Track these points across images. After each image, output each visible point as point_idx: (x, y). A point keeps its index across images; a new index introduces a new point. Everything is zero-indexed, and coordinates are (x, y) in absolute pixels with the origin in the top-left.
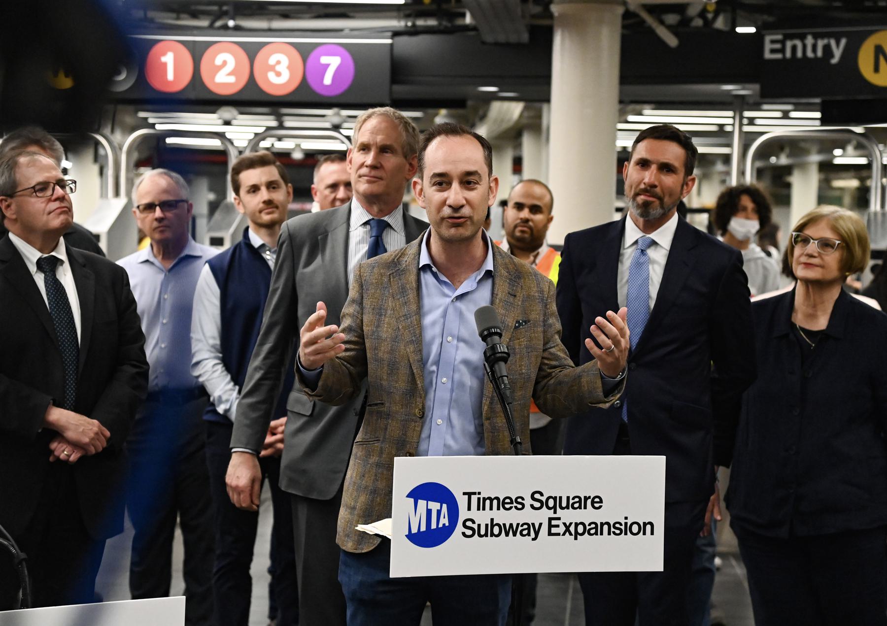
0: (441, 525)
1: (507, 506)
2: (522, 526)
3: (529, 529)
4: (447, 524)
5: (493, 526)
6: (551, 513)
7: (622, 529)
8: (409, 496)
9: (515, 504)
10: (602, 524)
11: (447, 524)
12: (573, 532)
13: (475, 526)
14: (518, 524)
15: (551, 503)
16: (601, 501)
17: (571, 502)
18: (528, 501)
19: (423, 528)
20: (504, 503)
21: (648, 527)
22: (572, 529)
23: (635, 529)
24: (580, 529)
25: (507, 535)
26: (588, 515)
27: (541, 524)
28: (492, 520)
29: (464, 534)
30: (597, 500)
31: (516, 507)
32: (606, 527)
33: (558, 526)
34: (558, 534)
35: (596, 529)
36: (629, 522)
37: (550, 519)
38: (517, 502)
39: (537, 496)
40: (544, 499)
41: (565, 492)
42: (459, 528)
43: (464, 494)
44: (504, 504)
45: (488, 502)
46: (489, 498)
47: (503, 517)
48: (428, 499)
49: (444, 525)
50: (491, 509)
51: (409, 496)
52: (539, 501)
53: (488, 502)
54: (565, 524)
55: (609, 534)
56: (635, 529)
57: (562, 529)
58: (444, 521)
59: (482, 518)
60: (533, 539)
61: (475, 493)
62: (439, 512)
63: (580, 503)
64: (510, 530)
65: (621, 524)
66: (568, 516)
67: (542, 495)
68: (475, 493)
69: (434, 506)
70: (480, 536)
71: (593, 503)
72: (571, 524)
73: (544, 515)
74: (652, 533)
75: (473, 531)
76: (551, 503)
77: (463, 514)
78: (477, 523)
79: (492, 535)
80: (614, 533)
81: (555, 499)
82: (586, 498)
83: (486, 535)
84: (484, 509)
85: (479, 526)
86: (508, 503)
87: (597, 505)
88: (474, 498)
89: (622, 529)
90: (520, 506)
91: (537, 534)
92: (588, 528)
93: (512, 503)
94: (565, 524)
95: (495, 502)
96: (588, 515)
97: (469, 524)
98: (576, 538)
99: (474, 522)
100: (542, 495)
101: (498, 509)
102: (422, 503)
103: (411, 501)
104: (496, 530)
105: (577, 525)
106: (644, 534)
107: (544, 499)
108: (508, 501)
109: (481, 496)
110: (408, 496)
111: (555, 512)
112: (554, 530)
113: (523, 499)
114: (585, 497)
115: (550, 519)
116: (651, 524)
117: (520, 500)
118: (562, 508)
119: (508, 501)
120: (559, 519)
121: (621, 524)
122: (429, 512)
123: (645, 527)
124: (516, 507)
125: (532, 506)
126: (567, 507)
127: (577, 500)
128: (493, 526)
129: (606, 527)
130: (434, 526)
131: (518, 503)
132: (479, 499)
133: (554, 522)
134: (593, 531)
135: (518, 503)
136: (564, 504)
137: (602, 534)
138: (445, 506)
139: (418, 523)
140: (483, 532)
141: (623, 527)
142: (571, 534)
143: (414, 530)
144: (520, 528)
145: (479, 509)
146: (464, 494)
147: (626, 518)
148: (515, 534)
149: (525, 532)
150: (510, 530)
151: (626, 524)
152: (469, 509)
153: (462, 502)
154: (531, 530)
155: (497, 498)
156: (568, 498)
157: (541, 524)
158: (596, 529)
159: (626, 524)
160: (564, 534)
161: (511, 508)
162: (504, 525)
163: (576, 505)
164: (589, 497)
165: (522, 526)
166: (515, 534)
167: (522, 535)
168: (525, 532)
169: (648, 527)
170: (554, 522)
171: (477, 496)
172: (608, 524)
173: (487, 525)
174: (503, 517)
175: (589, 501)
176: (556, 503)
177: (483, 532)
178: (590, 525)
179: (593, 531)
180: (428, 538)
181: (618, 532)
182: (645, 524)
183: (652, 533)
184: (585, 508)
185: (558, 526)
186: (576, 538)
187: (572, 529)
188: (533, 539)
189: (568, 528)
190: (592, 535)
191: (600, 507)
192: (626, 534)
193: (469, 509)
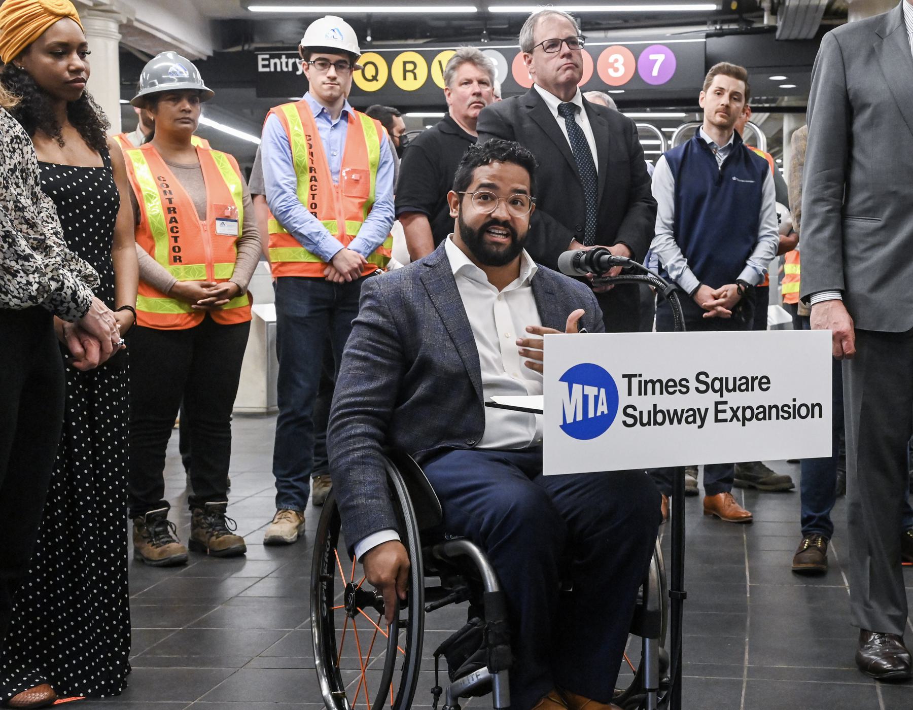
0: (599, 414)
1: (671, 390)
2: (687, 412)
3: (694, 415)
4: (606, 412)
5: (656, 413)
6: (717, 397)
7: (789, 412)
8: (562, 379)
9: (679, 388)
10: (770, 408)
11: (606, 412)
12: (741, 418)
13: (637, 414)
14: (683, 410)
15: (717, 385)
16: (768, 382)
17: (738, 383)
18: (693, 384)
19: (580, 417)
20: (667, 386)
21: (817, 409)
22: (740, 414)
23: (803, 411)
24: (748, 414)
25: (671, 422)
26: (755, 398)
27: (707, 410)
28: (655, 406)
29: (625, 423)
30: (764, 380)
31: (680, 391)
32: (774, 411)
33: (724, 411)
34: (725, 420)
35: (764, 413)
36: (798, 404)
37: (717, 404)
38: (681, 385)
39: (702, 377)
40: (709, 381)
41: (731, 372)
42: (620, 417)
43: (624, 376)
44: (667, 387)
45: (650, 385)
46: (652, 381)
47: (667, 402)
48: (584, 383)
49: (603, 412)
50: (654, 393)
51: (562, 379)
52: (705, 382)
53: (650, 385)
54: (732, 408)
55: (778, 418)
56: (803, 411)
57: (729, 414)
58: (603, 408)
59: (644, 404)
60: (700, 427)
61: (635, 376)
62: (597, 398)
63: (747, 384)
64: (674, 417)
65: (789, 407)
66: (735, 399)
67: (707, 376)
68: (635, 376)
69: (591, 391)
70: (643, 424)
71: (760, 383)
72: (738, 408)
73: (711, 398)
74: (820, 416)
75: (635, 420)
76: (717, 385)
77: (624, 400)
78: (639, 410)
79: (656, 423)
80: (782, 416)
81: (721, 380)
82: (753, 379)
83: (649, 423)
84: (646, 394)
85: (641, 413)
86: (671, 386)
87: (764, 386)
88: (635, 381)
89: (789, 412)
90: (684, 390)
91: (703, 420)
92: (756, 412)
93: (675, 386)
94: (732, 408)
95: (658, 385)
96: (755, 398)
97: (630, 411)
98: (744, 425)
99: (635, 409)
100: (707, 376)
101: (661, 393)
102: (577, 388)
103: (565, 385)
104: (660, 418)
105: (744, 409)
106: (813, 416)
107: (709, 381)
108: (671, 383)
109: (643, 379)
111: (722, 396)
112: (721, 416)
113: (688, 381)
114: (752, 377)
115: (717, 404)
116: (819, 405)
117: (684, 383)
118: (729, 391)
119: (671, 383)
120: (726, 403)
121: (789, 407)
122: (585, 398)
123: (813, 409)
124: (680, 391)
125: (697, 389)
126: (734, 390)
127: (744, 381)
128: (656, 413)
129: (774, 411)
130: (591, 415)
131: (682, 386)
132: (640, 382)
133: (720, 407)
134: (761, 416)
135: (682, 386)
136: (731, 387)
137: (770, 418)
138: (603, 391)
139: (574, 413)
140: (645, 420)
141: (791, 410)
142: (738, 420)
143: (570, 420)
144: (685, 415)
145: (640, 394)
146: (624, 376)
147: (794, 400)
149: (690, 419)
150: (674, 417)
151: (794, 406)
152: (630, 394)
153: (621, 385)
154: (697, 417)
155: (660, 381)
156: (735, 379)
157: (707, 410)
158: (764, 413)
159: (794, 406)
160: (731, 420)
161: (675, 391)
162: (668, 411)
163: (743, 387)
164: (757, 378)
166: (679, 422)
167: (687, 422)
168: (690, 419)
169: (817, 409)
170: (720, 407)
171: (638, 379)
172: (776, 407)
173: (649, 412)
174: (667, 402)
175: (756, 382)
176: (722, 386)
177: (645, 420)
178: (757, 409)
179: (761, 416)
180: (585, 428)
181: (786, 415)
182: (813, 406)
183: (820, 416)
184: (753, 390)
185: (724, 411)
186: (744, 425)
187: (740, 414)
188: (700, 427)
189: (735, 412)
190: (760, 420)
191: (768, 388)
192: (794, 417)
193: (630, 394)
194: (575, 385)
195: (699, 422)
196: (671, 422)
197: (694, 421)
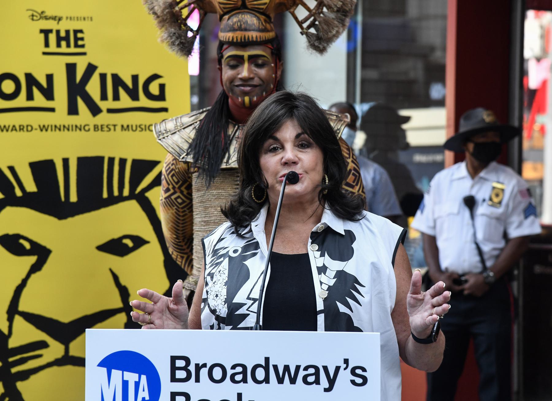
2: (306, 369)
3: (317, 374)
4: (147, 398)
8: (101, 365)
14: (298, 368)
48: (124, 369)
51: (101, 365)
60: (326, 390)
62: (137, 384)
69: (132, 377)
91: (332, 382)
102: (116, 374)
103: (104, 370)
110: (99, 365)
122: (125, 384)
138: (144, 377)
144: (302, 373)
148: (293, 381)
149: (311, 379)
165: (306, 369)
166: (293, 381)
188: (326, 390)
194: (114, 372)
195: (324, 383)
196: (281, 381)
197: (317, 382)
